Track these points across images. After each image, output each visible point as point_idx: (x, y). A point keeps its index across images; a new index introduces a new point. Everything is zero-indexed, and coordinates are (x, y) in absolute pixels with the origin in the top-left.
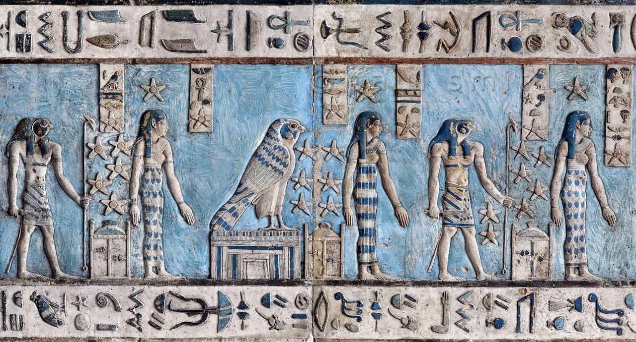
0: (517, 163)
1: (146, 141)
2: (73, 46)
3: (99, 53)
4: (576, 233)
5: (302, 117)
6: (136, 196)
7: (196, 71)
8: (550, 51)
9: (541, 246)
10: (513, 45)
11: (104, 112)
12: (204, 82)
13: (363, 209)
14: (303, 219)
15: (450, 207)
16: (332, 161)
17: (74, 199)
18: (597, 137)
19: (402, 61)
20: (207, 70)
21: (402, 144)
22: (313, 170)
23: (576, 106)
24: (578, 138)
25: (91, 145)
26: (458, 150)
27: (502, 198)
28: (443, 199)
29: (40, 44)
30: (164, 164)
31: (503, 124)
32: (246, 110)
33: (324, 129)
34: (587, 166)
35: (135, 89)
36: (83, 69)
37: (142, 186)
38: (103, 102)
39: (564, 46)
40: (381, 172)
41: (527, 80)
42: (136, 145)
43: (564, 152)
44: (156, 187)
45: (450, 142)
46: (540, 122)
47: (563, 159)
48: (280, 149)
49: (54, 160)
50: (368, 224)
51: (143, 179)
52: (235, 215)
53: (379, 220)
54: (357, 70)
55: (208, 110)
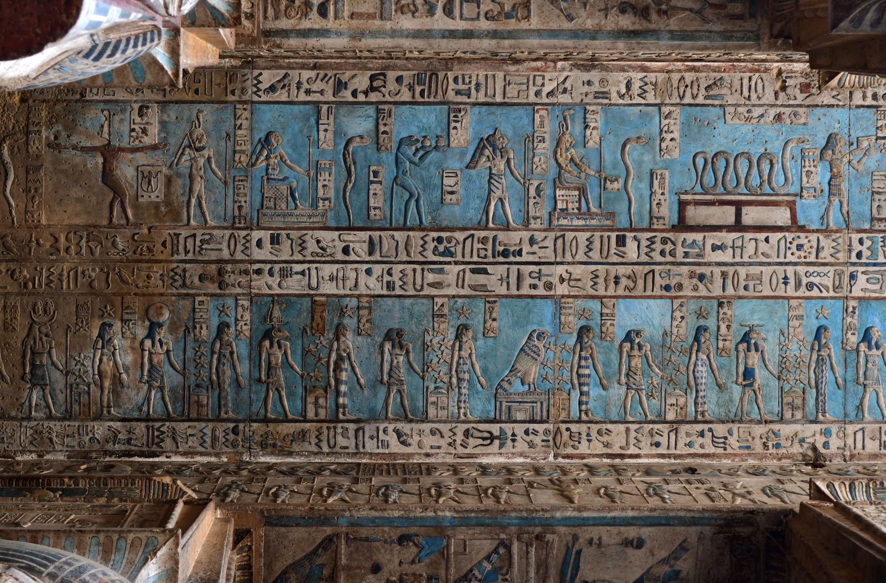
0: (669, 354)
1: (460, 342)
2: (419, 288)
3: (434, 292)
4: (701, 394)
5: (548, 328)
6: (454, 372)
7: (489, 302)
8: (687, 292)
9: (682, 401)
10: (667, 288)
11: (436, 325)
12: (493, 308)
13: (582, 380)
14: (548, 386)
15: (631, 379)
16: (565, 353)
17: (418, 374)
18: (713, 340)
19: (605, 297)
20: (495, 302)
21: (604, 343)
22: (554, 359)
23: (702, 322)
24: (703, 340)
25: (429, 344)
26: (636, 347)
27: (660, 374)
28: (627, 375)
29: (400, 286)
30: (470, 355)
31: (661, 332)
32: (517, 324)
33: (560, 335)
34: (708, 356)
35: (454, 312)
36: (425, 301)
37: (457, 367)
38: (435, 319)
39: (696, 289)
40: (593, 359)
41: (675, 307)
42: (454, 344)
43: (695, 348)
44: (465, 368)
45: (632, 342)
46: (682, 331)
47: (694, 352)
48: (536, 346)
49: (408, 352)
50: (585, 389)
51: (458, 363)
52: (510, 384)
53: (591, 386)
54: (579, 302)
55: (495, 324)
